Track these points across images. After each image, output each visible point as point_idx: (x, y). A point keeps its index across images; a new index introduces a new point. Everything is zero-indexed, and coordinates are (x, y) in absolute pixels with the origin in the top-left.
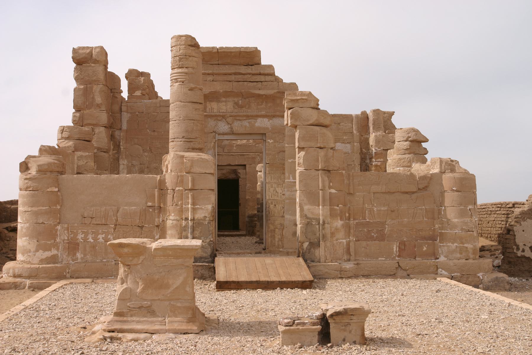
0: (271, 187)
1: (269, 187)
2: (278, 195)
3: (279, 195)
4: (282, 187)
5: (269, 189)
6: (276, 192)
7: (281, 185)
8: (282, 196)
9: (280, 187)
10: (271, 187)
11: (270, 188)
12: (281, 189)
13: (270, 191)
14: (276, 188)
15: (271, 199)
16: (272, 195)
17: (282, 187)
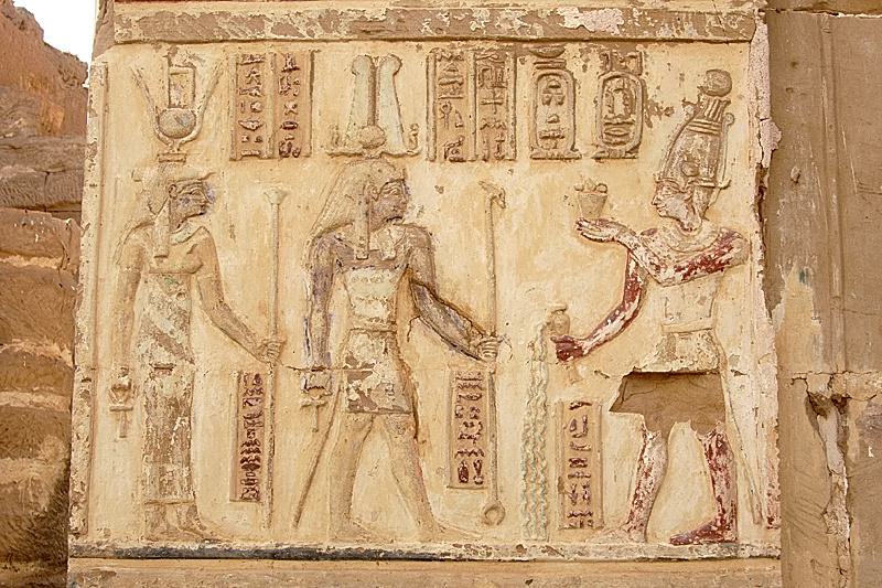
0: (246, 148)
1: (176, 136)
2: (473, 397)
3: (511, 412)
4: (618, 142)
5: (192, 199)
6: (421, 289)
7: (585, 69)
8: (621, 433)
9: (553, 147)
10: (246, 148)
11: (208, 156)
12: (594, 224)
13: (198, 268)
14: (424, 177)
15: (242, 525)
16: (289, 392)
17: (618, 142)
